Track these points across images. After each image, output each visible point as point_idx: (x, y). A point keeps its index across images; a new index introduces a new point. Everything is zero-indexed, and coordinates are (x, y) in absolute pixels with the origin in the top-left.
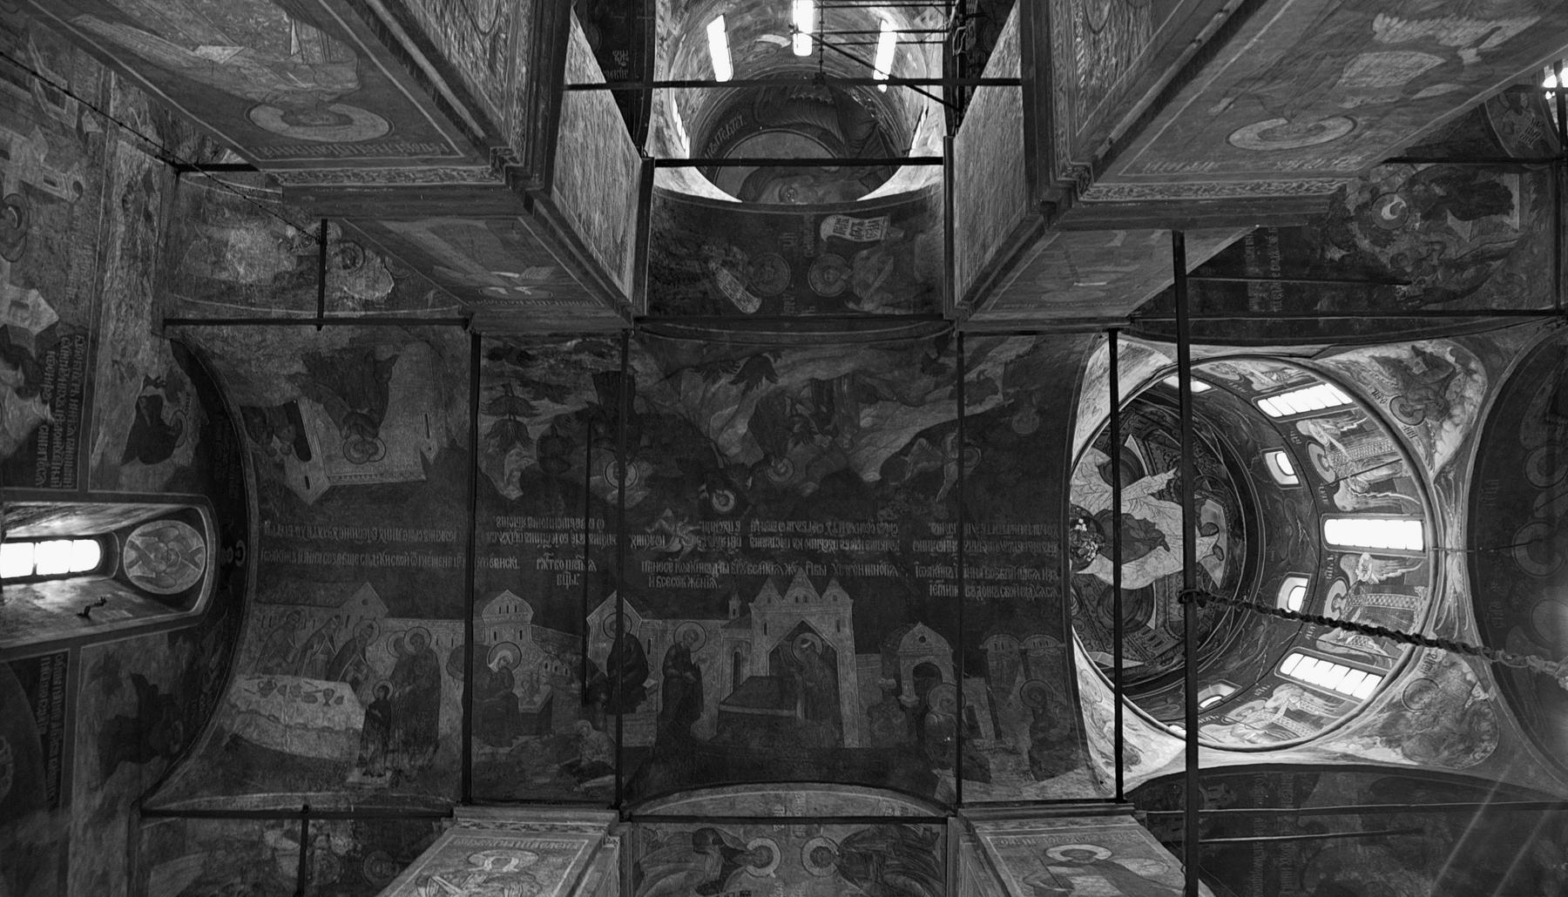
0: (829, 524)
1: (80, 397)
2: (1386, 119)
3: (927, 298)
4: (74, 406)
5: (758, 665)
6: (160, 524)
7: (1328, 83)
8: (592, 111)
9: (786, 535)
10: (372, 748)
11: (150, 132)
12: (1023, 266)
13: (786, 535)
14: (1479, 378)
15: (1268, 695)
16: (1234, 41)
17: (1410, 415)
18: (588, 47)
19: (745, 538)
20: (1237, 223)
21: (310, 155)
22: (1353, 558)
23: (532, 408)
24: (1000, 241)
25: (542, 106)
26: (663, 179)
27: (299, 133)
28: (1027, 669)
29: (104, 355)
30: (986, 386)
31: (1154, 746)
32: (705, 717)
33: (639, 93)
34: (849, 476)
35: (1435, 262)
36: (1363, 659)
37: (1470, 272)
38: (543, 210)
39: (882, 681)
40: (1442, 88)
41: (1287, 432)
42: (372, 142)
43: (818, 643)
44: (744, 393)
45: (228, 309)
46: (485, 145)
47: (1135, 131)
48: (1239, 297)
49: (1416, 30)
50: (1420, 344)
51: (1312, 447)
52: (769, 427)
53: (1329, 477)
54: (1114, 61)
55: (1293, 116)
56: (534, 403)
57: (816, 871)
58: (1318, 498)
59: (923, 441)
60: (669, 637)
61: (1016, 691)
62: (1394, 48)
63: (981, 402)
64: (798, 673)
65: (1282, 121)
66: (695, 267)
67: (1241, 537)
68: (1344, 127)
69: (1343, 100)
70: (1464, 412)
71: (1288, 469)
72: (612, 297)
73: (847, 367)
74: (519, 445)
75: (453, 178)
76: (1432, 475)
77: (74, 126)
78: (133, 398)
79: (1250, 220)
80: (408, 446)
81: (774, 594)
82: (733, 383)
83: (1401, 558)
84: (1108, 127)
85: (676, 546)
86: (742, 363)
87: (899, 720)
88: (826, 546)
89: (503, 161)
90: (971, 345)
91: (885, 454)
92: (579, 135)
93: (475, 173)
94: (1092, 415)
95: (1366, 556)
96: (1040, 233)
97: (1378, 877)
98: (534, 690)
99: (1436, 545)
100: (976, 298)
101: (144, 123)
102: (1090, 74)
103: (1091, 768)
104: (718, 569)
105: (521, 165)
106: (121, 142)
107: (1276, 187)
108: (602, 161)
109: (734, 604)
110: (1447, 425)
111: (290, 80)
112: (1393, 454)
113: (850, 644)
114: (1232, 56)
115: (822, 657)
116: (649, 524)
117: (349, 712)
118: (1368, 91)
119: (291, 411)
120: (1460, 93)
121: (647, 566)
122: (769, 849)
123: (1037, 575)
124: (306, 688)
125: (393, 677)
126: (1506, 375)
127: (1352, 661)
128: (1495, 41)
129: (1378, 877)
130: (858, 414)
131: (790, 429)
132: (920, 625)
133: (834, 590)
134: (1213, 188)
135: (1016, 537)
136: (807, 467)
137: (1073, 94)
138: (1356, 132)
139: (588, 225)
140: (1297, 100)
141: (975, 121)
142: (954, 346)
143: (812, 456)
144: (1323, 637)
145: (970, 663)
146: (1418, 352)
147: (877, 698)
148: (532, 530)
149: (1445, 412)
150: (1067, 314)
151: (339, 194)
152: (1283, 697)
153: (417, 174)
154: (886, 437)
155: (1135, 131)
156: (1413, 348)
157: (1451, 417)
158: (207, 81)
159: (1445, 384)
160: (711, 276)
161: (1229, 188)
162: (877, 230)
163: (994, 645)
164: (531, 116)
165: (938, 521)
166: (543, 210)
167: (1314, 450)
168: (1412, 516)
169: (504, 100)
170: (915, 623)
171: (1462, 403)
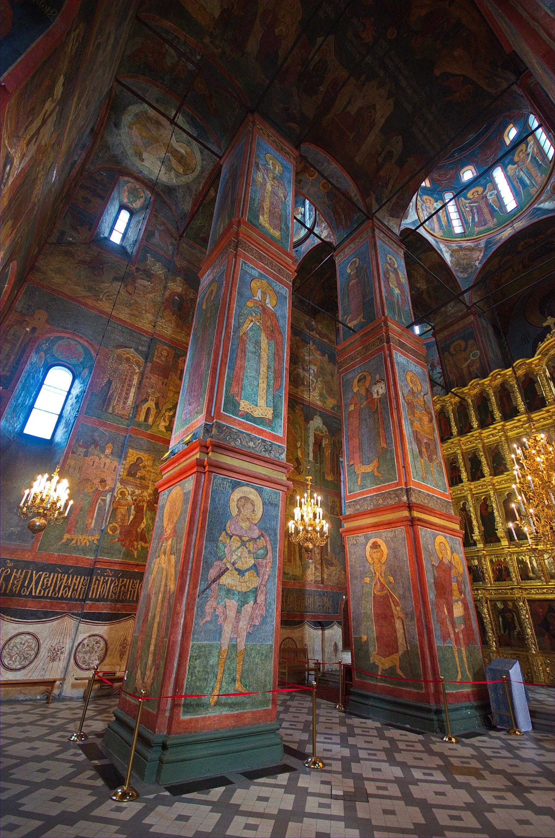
5: (353, 110)
36: (465, 220)
57: (321, 188)
58: (505, 156)
76: (536, 206)
83: (502, 206)
95: (496, 192)
109: (363, 77)
113: (381, 125)
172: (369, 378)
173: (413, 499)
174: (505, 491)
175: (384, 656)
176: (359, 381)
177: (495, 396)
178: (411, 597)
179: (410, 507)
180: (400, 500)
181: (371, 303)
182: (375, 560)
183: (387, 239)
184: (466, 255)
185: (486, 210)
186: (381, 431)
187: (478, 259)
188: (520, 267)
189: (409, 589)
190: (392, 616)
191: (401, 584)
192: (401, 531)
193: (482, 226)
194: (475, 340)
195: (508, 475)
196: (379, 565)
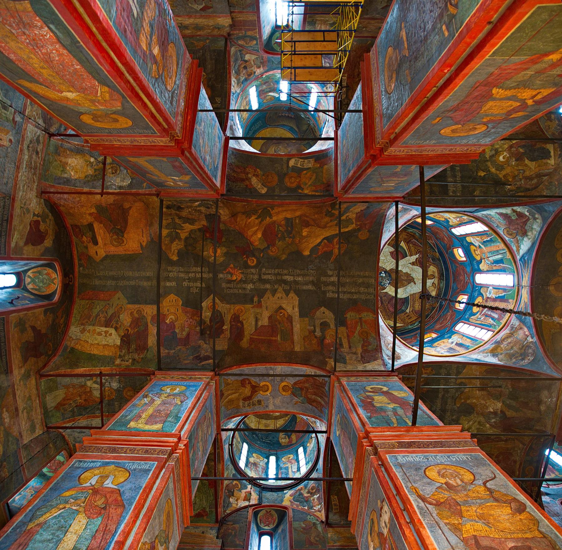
0: (291, 270)
1: (7, 220)
2: (500, 125)
3: (328, 188)
4: (5, 224)
5: (264, 321)
6: (39, 269)
7: (477, 112)
8: (207, 120)
9: (275, 274)
10: (124, 351)
11: (41, 122)
12: (363, 178)
13: (275, 274)
15: (450, 337)
16: (441, 98)
18: (206, 96)
19: (260, 275)
20: (444, 163)
21: (102, 133)
22: (486, 289)
23: (182, 227)
24: (355, 169)
25: (189, 117)
26: (232, 144)
27: (98, 125)
28: (361, 324)
29: (17, 204)
30: (349, 221)
31: (406, 353)
32: (245, 340)
33: (224, 113)
34: (298, 253)
35: (521, 177)
36: (487, 326)
37: (535, 181)
38: (188, 155)
39: (309, 328)
40: (520, 114)
41: (462, 241)
42: (125, 129)
43: (286, 313)
44: (260, 223)
45: (67, 188)
46: (167, 131)
47: (405, 129)
48: (444, 190)
49: (509, 93)
50: (515, 208)
51: (472, 247)
52: (270, 234)
53: (478, 258)
54: (396, 104)
55: (464, 124)
56: (183, 225)
59: (326, 241)
60: (232, 311)
61: (357, 332)
62: (501, 99)
63: (347, 227)
64: (278, 324)
65: (460, 126)
66: (243, 176)
67: (443, 280)
68: (482, 129)
69: (483, 118)
71: (462, 254)
72: (212, 186)
73: (298, 213)
74: (177, 240)
75: (155, 142)
77: (11, 119)
78: (28, 221)
79: (449, 162)
80: (135, 240)
81: (270, 296)
82: (256, 219)
83: (504, 289)
84: (394, 128)
85: (234, 278)
86: (260, 211)
87: (314, 341)
88: (289, 278)
89: (174, 137)
90: (344, 206)
91: (311, 246)
92: (202, 128)
93: (163, 141)
94: (388, 232)
96: (369, 166)
97: (483, 402)
98: (182, 330)
100: (346, 189)
101: (39, 118)
102: (388, 109)
103: (383, 360)
104: (250, 286)
105: (181, 138)
106: (29, 125)
107: (458, 150)
108: (210, 137)
109: (256, 299)
111: (96, 105)
112: (503, 250)
113: (298, 314)
114: (440, 103)
115: (287, 319)
116: (225, 269)
117: (115, 339)
118: (492, 115)
119: (90, 226)
120: (528, 116)
121: (224, 285)
122: (268, 386)
123: (366, 290)
124: (98, 330)
125: (130, 326)
127: (482, 326)
128: (539, 97)
129: (483, 402)
130: (302, 230)
131: (277, 236)
132: (323, 308)
133: (292, 294)
134: (434, 150)
135: (359, 276)
136: (283, 250)
137: (381, 116)
138: (488, 130)
139: (205, 160)
140: (465, 118)
141: (346, 125)
142: (337, 206)
143: (285, 246)
144: (472, 317)
145: (341, 322)
146: (514, 211)
147: (307, 334)
148: (181, 272)
150: (380, 195)
151: (112, 147)
152: (455, 338)
153: (142, 141)
154: (312, 239)
155: (405, 129)
156: (512, 209)
158: (65, 105)
160: (249, 179)
161: (439, 151)
162: (310, 164)
163: (350, 315)
164: (185, 121)
165: (330, 270)
166: (188, 155)
167: (472, 248)
169: (176, 115)
170: (321, 307)
183: (361, 378)
184: (510, 343)
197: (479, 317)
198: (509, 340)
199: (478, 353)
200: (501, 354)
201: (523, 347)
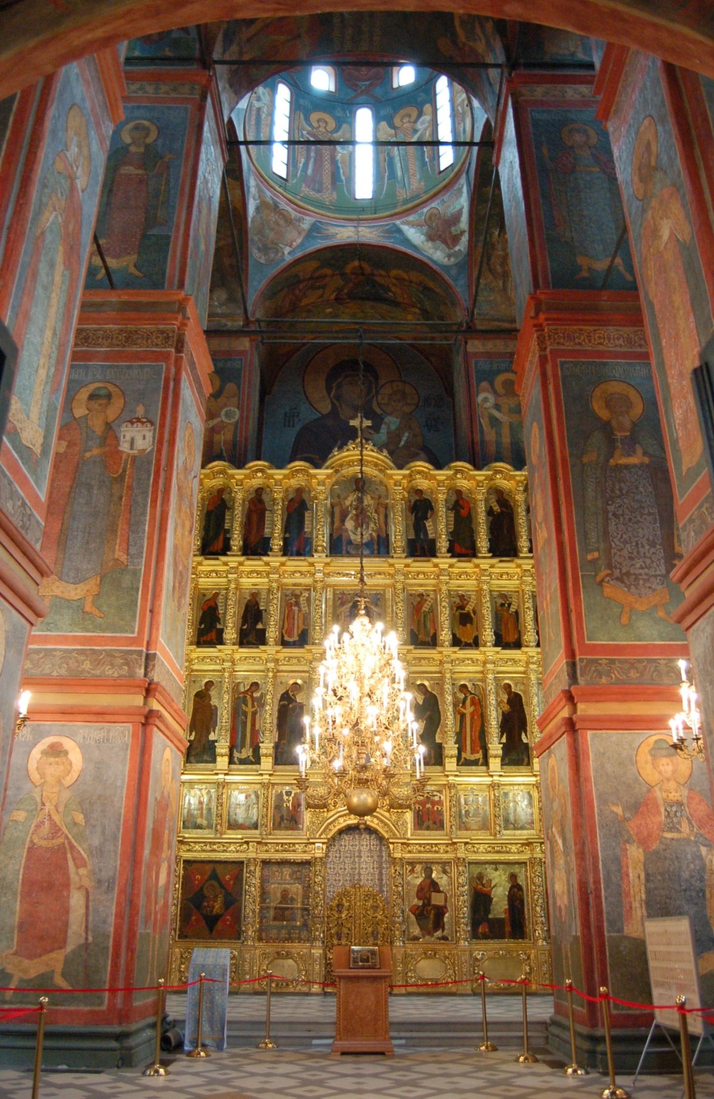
14: (445, 261)
17: (430, 218)
36: (294, 158)
51: (415, 114)
53: (397, 121)
70: (429, 248)
76: (398, 222)
83: (350, 179)
99: (360, 220)
110: (423, 238)
126: (446, 277)
144: (302, 117)
146: (462, 232)
149: (430, 238)
157: (427, 241)
159: (445, 242)
168: (375, 192)
171: (434, 248)
172: (117, 404)
173: (156, 676)
174: (204, 677)
175: (30, 957)
176: (92, 397)
177: (243, 505)
178: (115, 852)
179: (149, 690)
180: (132, 675)
181: (163, 243)
182: (49, 779)
184: (278, 225)
185: (327, 165)
186: (121, 525)
187: (292, 247)
188: (333, 296)
189: (115, 838)
190: (67, 885)
191: (99, 829)
192: (123, 733)
193: (314, 190)
194: (239, 387)
195: (220, 651)
196: (56, 790)
197: (305, 133)
198: (282, 222)
199: (257, 185)
200: (261, 218)
201: (276, 244)
